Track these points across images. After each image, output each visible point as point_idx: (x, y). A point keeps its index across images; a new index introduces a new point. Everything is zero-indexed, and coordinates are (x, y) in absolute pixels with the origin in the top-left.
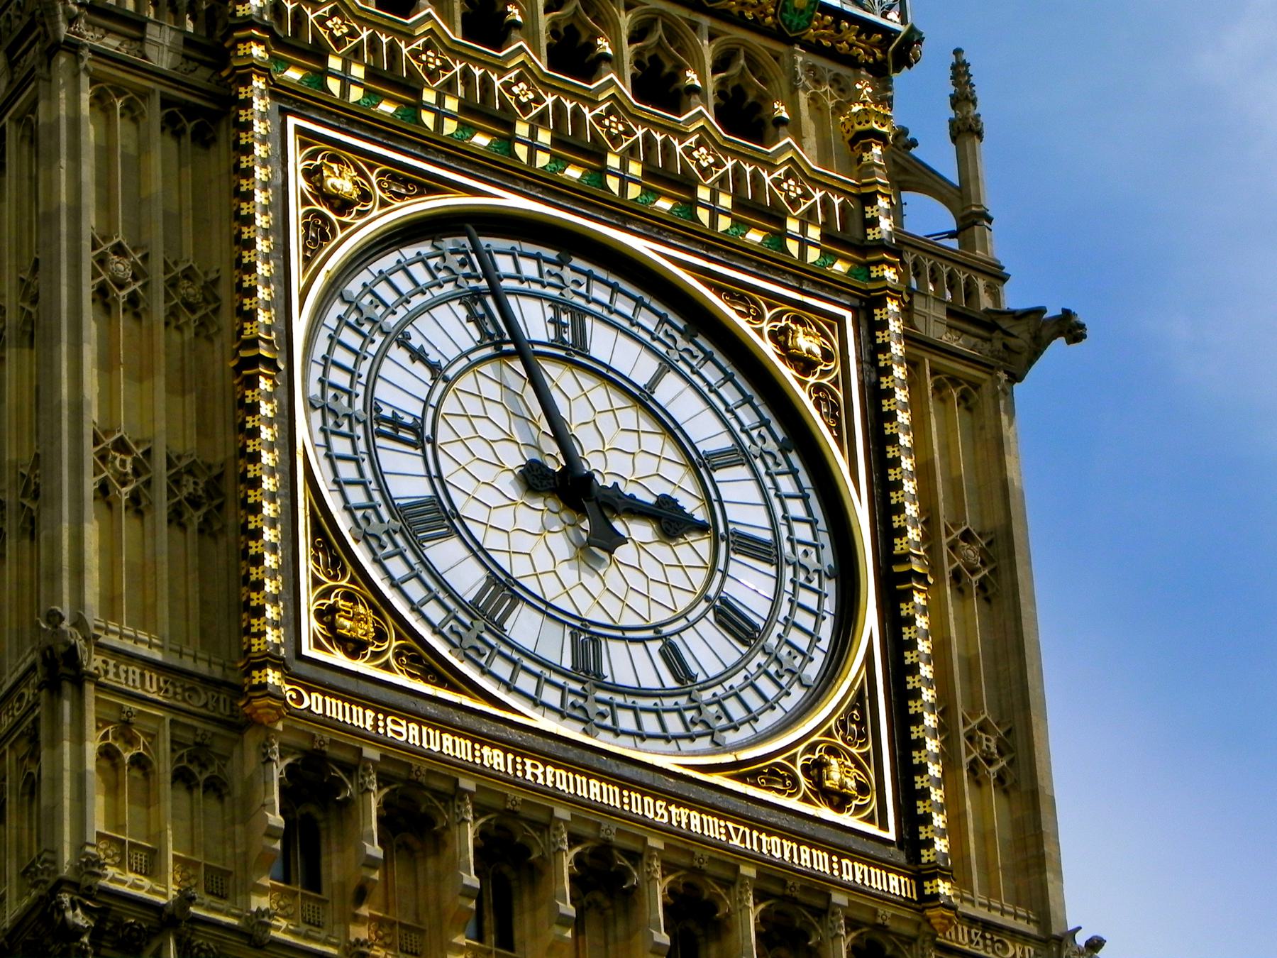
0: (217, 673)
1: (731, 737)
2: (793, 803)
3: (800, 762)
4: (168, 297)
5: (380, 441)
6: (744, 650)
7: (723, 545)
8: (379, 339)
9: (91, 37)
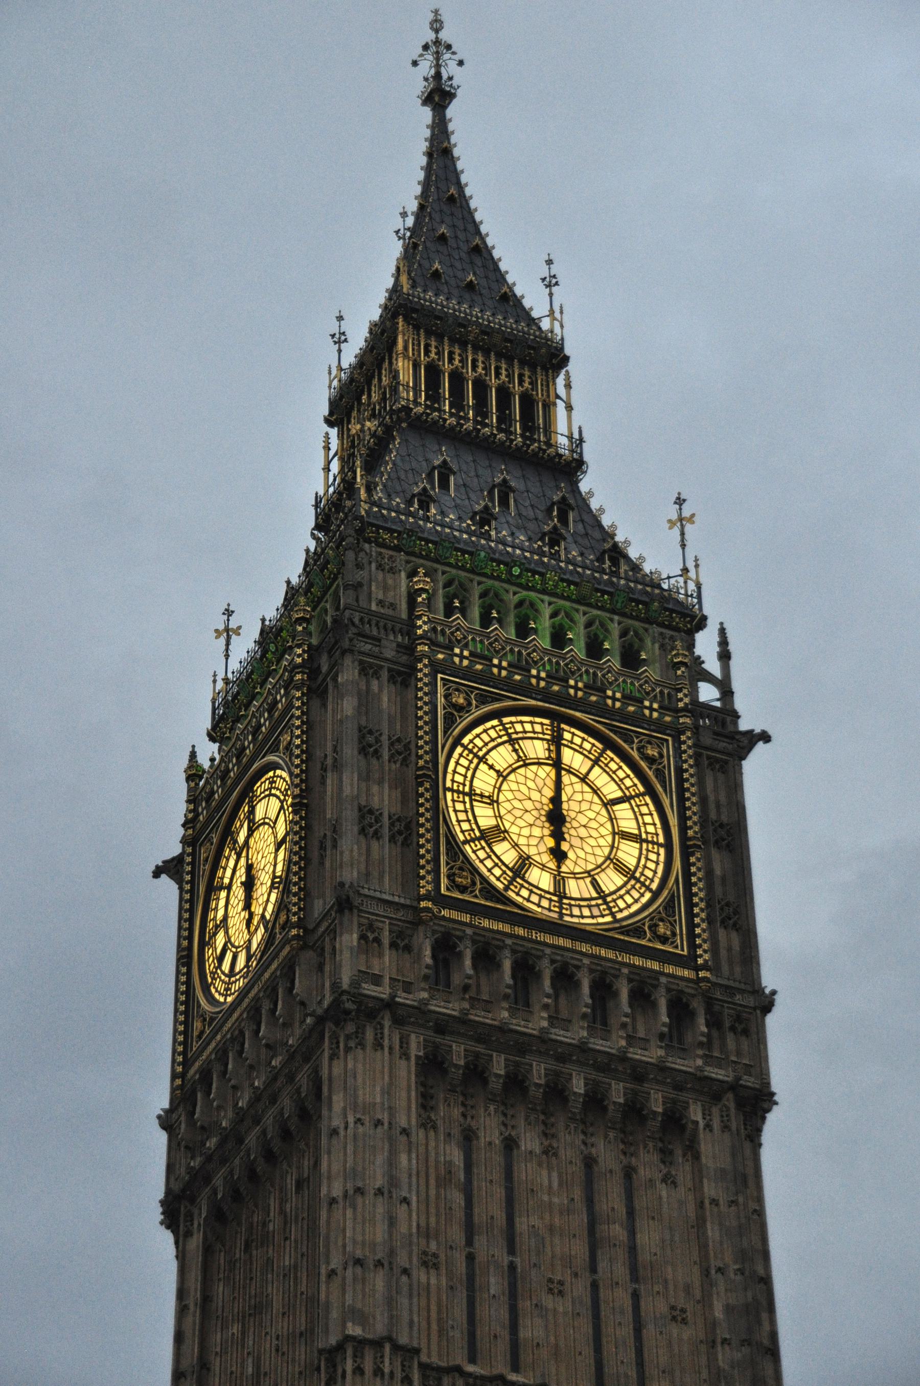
0: (408, 902)
3: (647, 925)
4: (390, 750)
5: (475, 803)
6: (625, 879)
7: (617, 837)
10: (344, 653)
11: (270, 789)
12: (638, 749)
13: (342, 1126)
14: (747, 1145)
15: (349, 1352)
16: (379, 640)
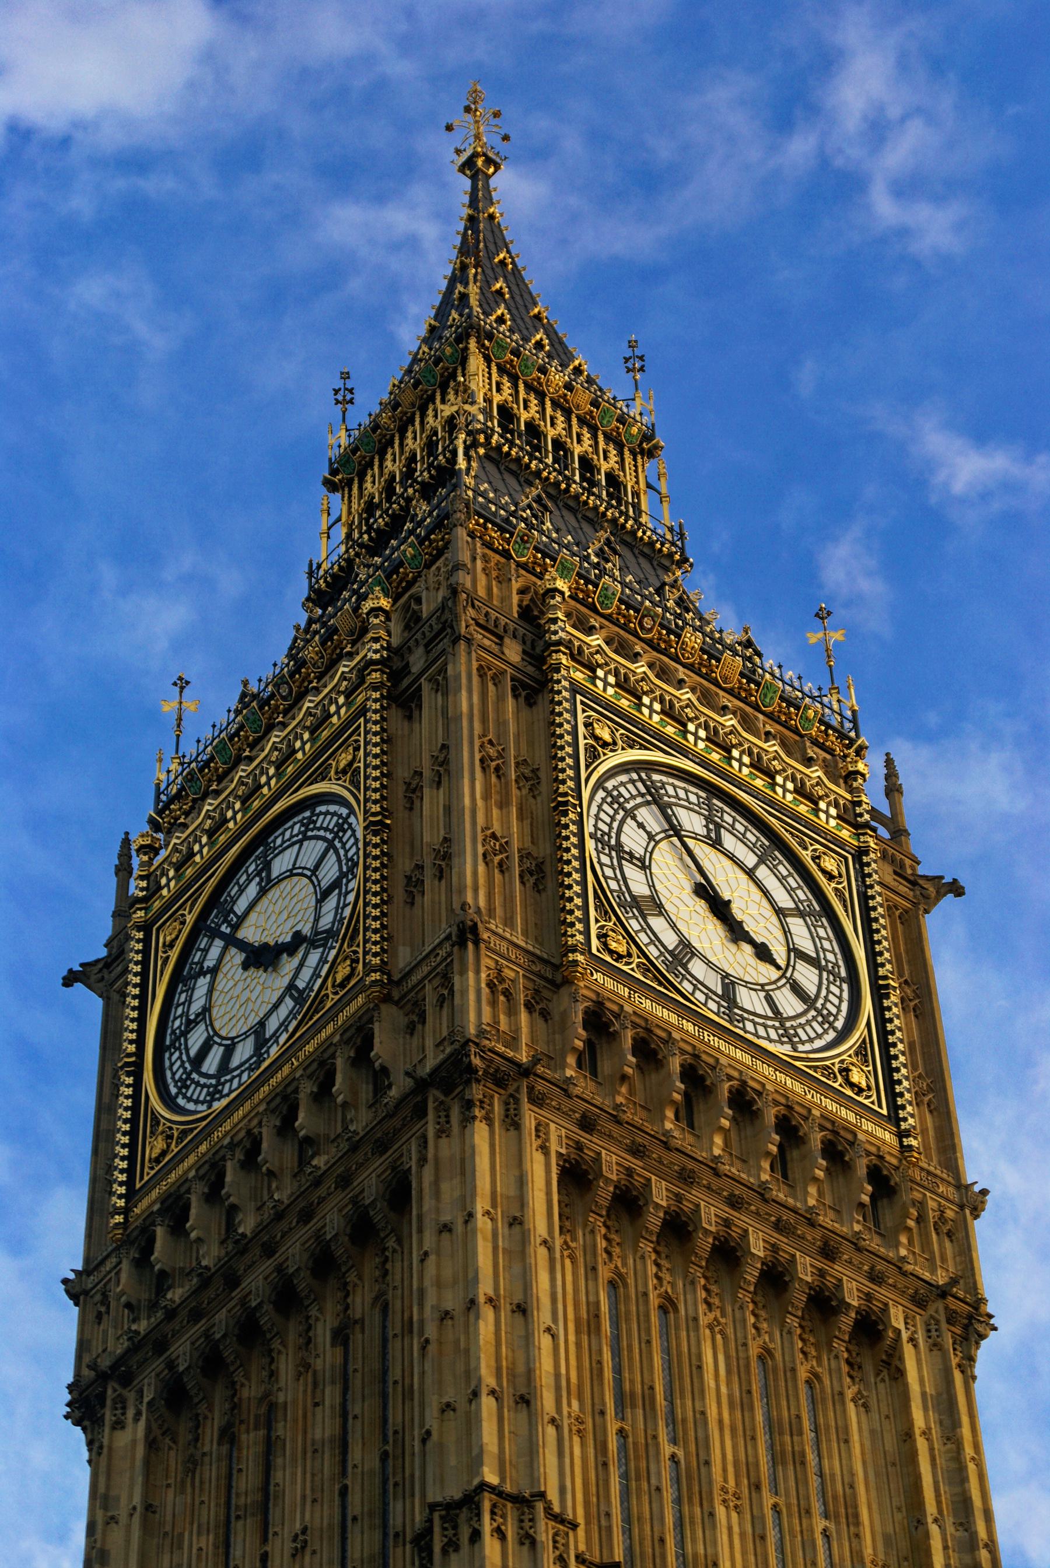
0: (545, 956)
1: (801, 1048)
2: (836, 1085)
8: (622, 813)
10: (456, 640)
11: (304, 833)
12: (813, 859)
13: (460, 1221)
15: (487, 1506)
16: (501, 638)
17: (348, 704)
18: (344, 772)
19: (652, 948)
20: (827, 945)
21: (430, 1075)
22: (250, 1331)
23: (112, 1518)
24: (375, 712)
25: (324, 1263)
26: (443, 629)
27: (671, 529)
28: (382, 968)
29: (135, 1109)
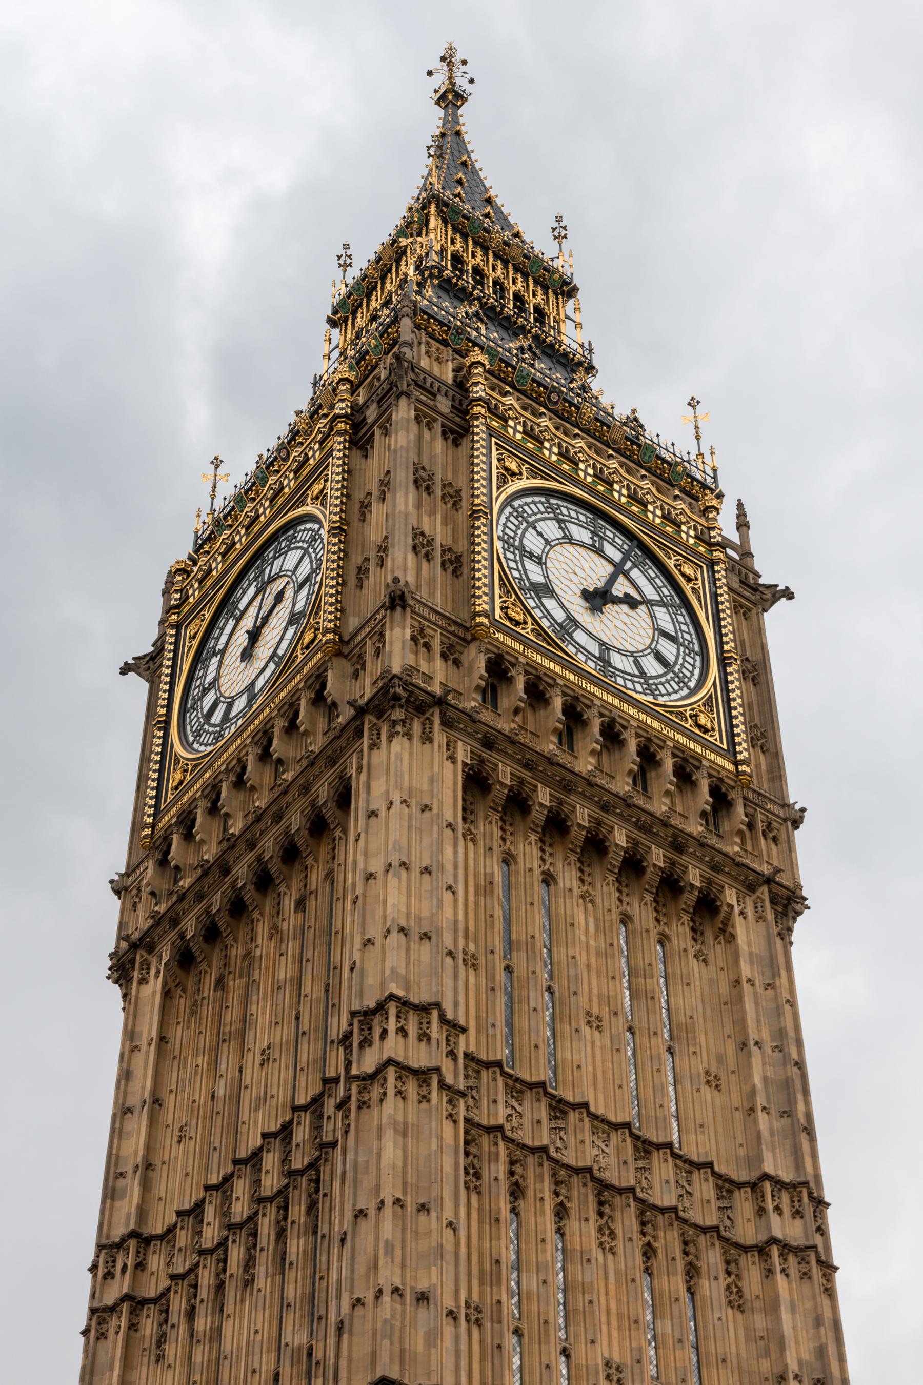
1: (660, 698)
2: (687, 726)
8: (525, 524)
9: (417, 393)
10: (398, 397)
12: (676, 566)
14: (778, 941)
16: (435, 395)
17: (321, 449)
18: (317, 498)
19: (544, 620)
20: (684, 628)
21: (367, 704)
22: (238, 908)
23: (136, 1047)
24: (339, 451)
25: (291, 854)
26: (391, 389)
27: (582, 346)
28: (335, 630)
29: (163, 754)
